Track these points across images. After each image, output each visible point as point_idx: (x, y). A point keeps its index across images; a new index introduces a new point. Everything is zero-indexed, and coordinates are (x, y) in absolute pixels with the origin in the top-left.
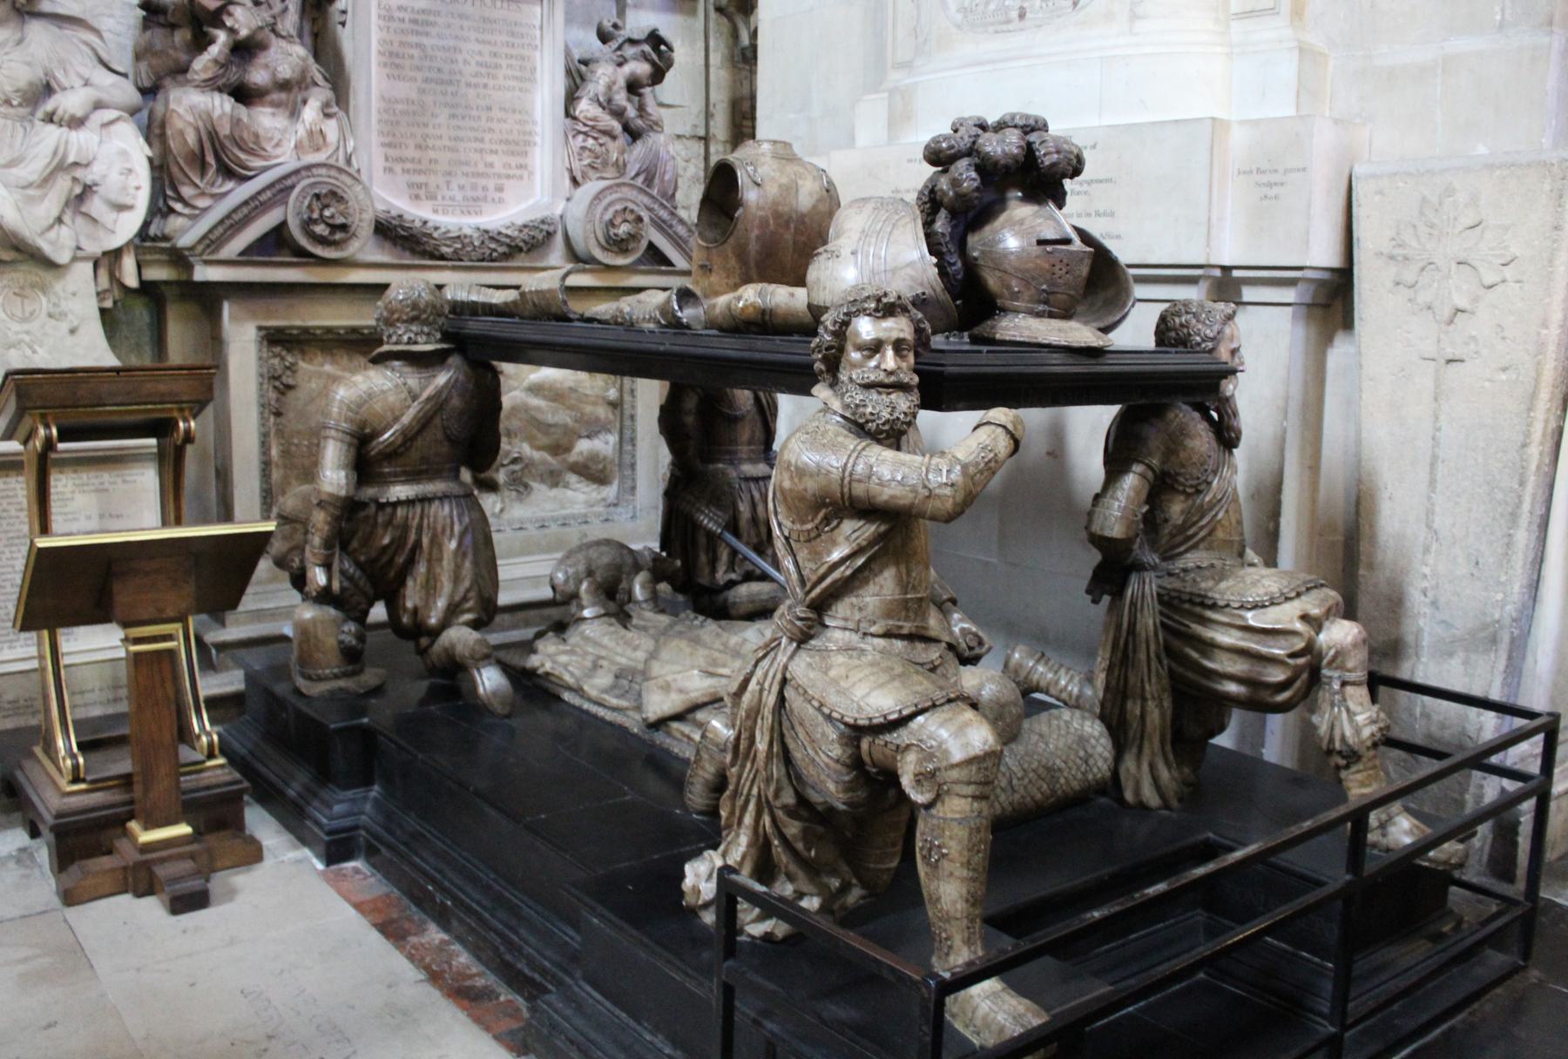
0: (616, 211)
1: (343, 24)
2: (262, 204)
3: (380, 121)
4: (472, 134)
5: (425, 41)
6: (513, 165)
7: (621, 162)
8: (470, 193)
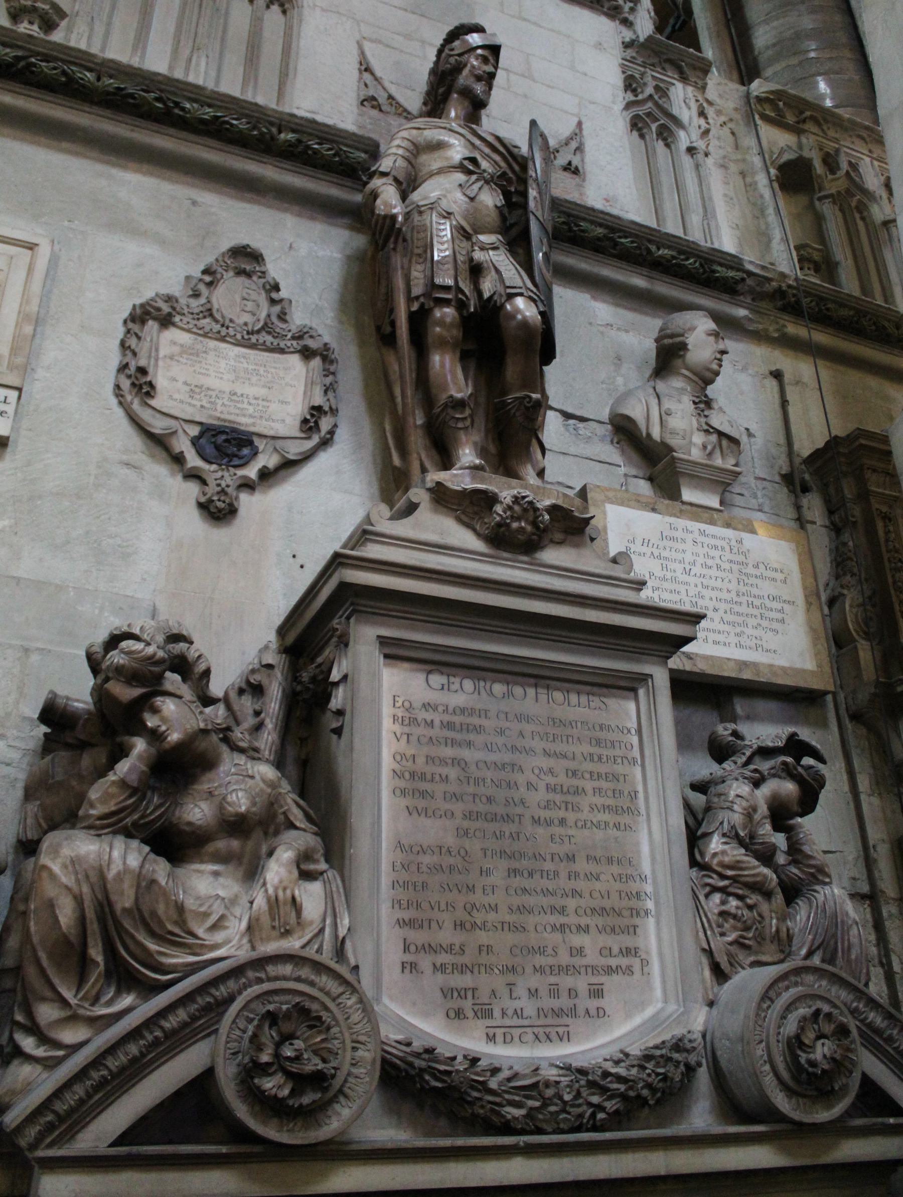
0: (804, 1019)
2: (169, 1035)
4: (546, 901)
5: (466, 754)
6: (615, 950)
7: (783, 934)
8: (549, 1003)
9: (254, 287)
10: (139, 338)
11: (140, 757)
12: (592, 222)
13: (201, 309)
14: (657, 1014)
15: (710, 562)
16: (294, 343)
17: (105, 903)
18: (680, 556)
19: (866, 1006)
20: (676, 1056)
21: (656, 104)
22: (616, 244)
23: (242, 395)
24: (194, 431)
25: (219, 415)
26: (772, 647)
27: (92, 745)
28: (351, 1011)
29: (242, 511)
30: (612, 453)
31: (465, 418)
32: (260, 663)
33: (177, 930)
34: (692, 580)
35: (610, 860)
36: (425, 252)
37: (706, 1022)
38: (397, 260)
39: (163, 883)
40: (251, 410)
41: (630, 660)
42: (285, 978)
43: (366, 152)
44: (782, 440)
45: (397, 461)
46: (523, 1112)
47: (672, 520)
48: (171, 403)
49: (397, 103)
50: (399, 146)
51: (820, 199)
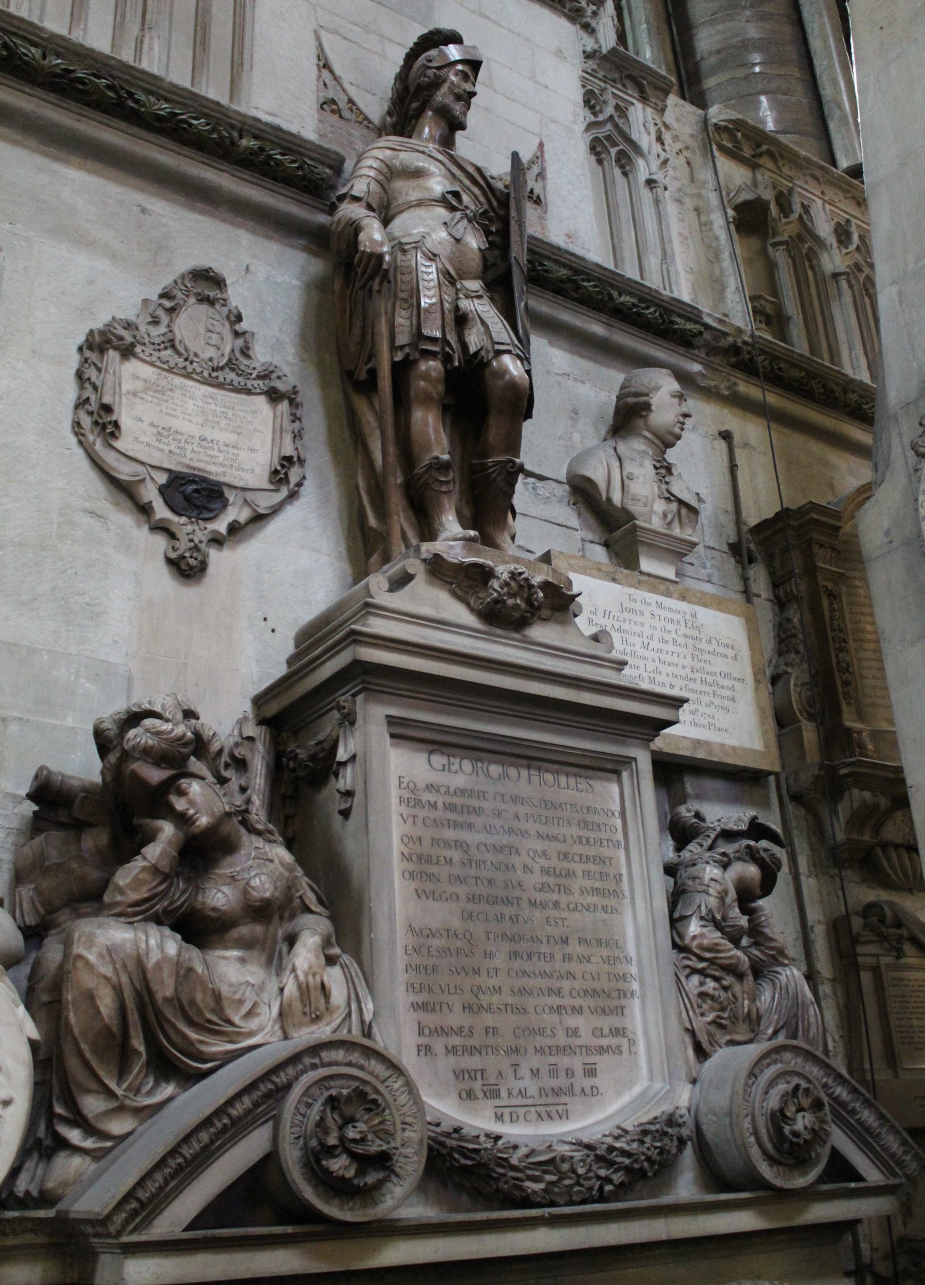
0: (785, 1094)
1: (345, 814)
2: (235, 1122)
3: (408, 967)
4: (544, 983)
5: (466, 836)
7: (754, 1015)
8: (550, 1083)
9: (217, 317)
10: (99, 370)
11: (170, 842)
12: (556, 262)
13: (162, 339)
14: (645, 1091)
15: (667, 637)
16: (261, 382)
17: (145, 993)
18: (638, 629)
19: (834, 1081)
20: (670, 1130)
21: (616, 126)
22: (578, 287)
23: (212, 441)
24: (162, 479)
25: (188, 462)
26: (724, 725)
27: (91, 825)
28: (397, 1094)
29: (211, 569)
30: (568, 515)
31: (447, 482)
32: (241, 735)
33: (215, 1019)
34: (650, 654)
35: (599, 943)
36: (412, 297)
37: (690, 1099)
38: (382, 305)
39: (200, 971)
40: (221, 458)
41: (615, 742)
42: (337, 1064)
43: (331, 167)
44: (730, 507)
45: (372, 521)
46: (542, 1186)
47: (631, 591)
48: (137, 447)
49: (358, 109)
50: (371, 167)
51: (774, 245)
